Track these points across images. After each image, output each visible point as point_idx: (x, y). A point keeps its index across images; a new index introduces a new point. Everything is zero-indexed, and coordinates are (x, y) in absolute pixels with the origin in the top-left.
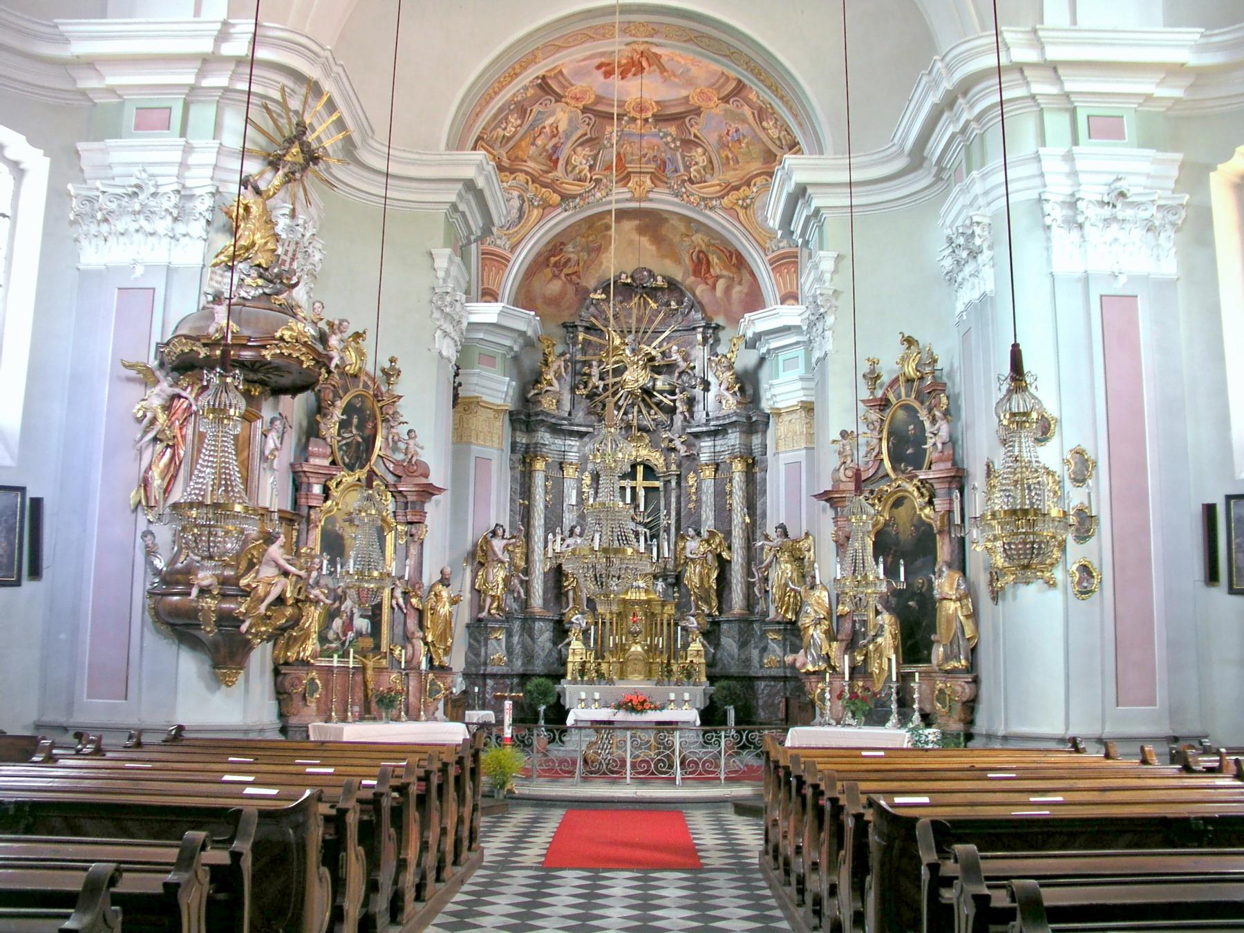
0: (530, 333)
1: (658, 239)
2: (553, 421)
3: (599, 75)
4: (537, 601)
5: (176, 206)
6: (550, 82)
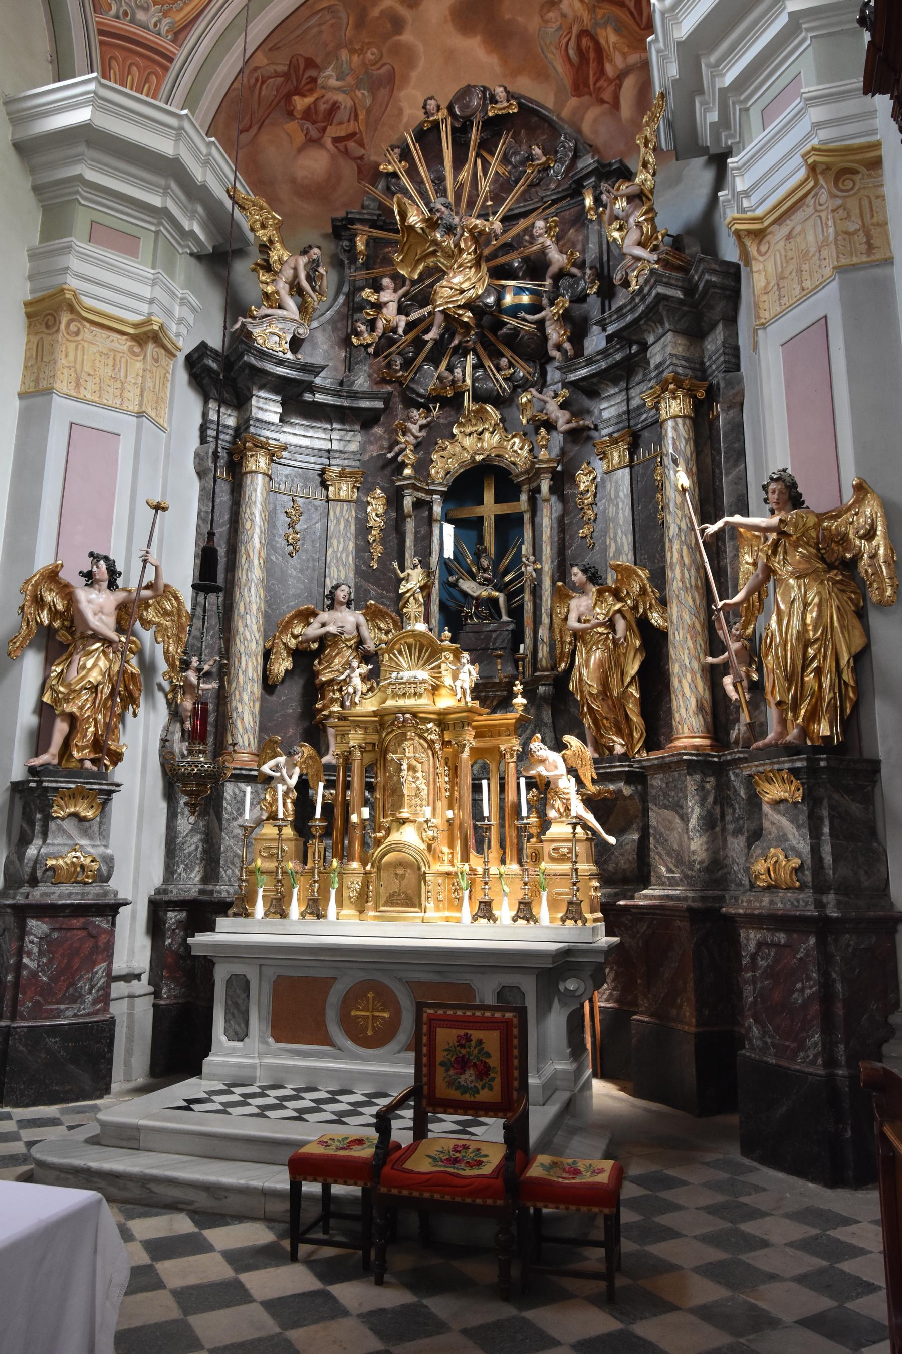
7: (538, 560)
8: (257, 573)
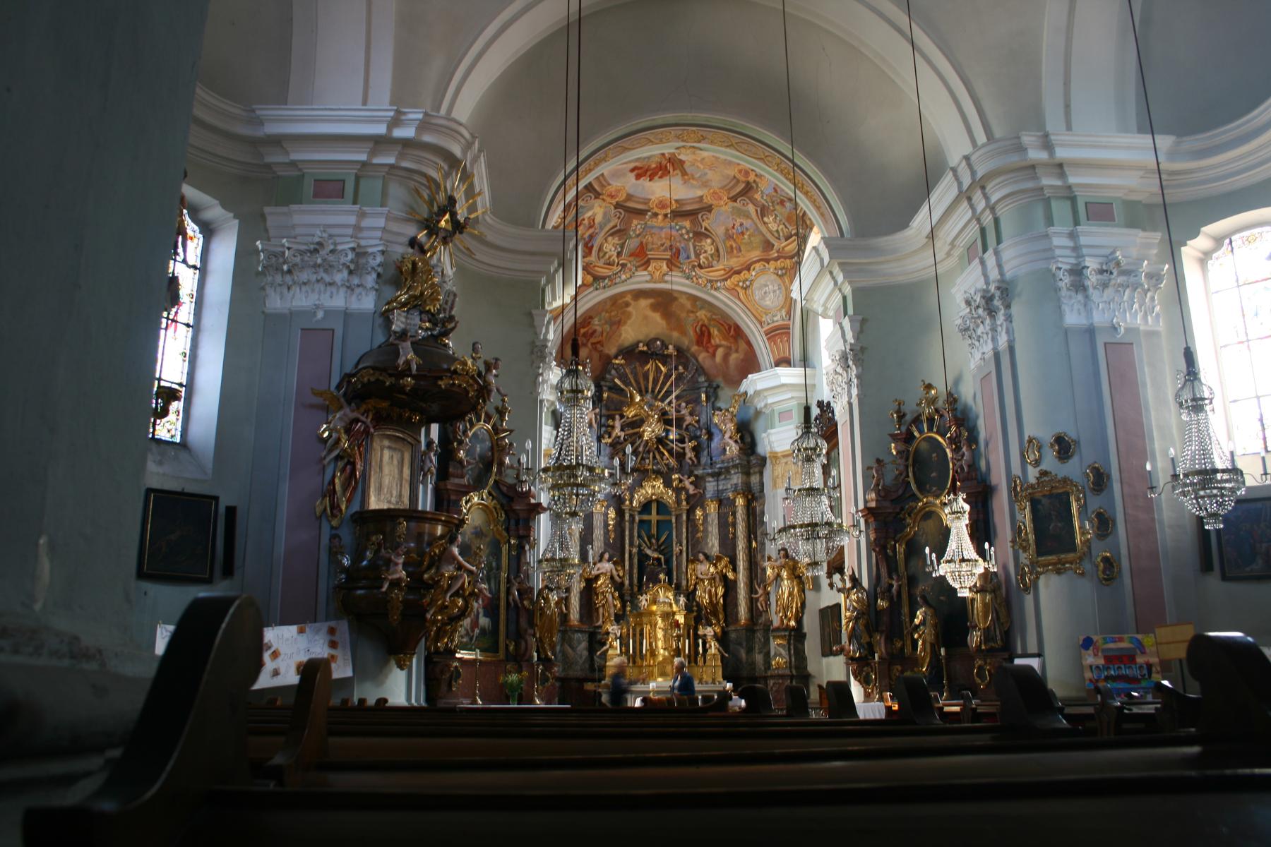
3: (632, 176)
4: (574, 615)
5: (352, 261)
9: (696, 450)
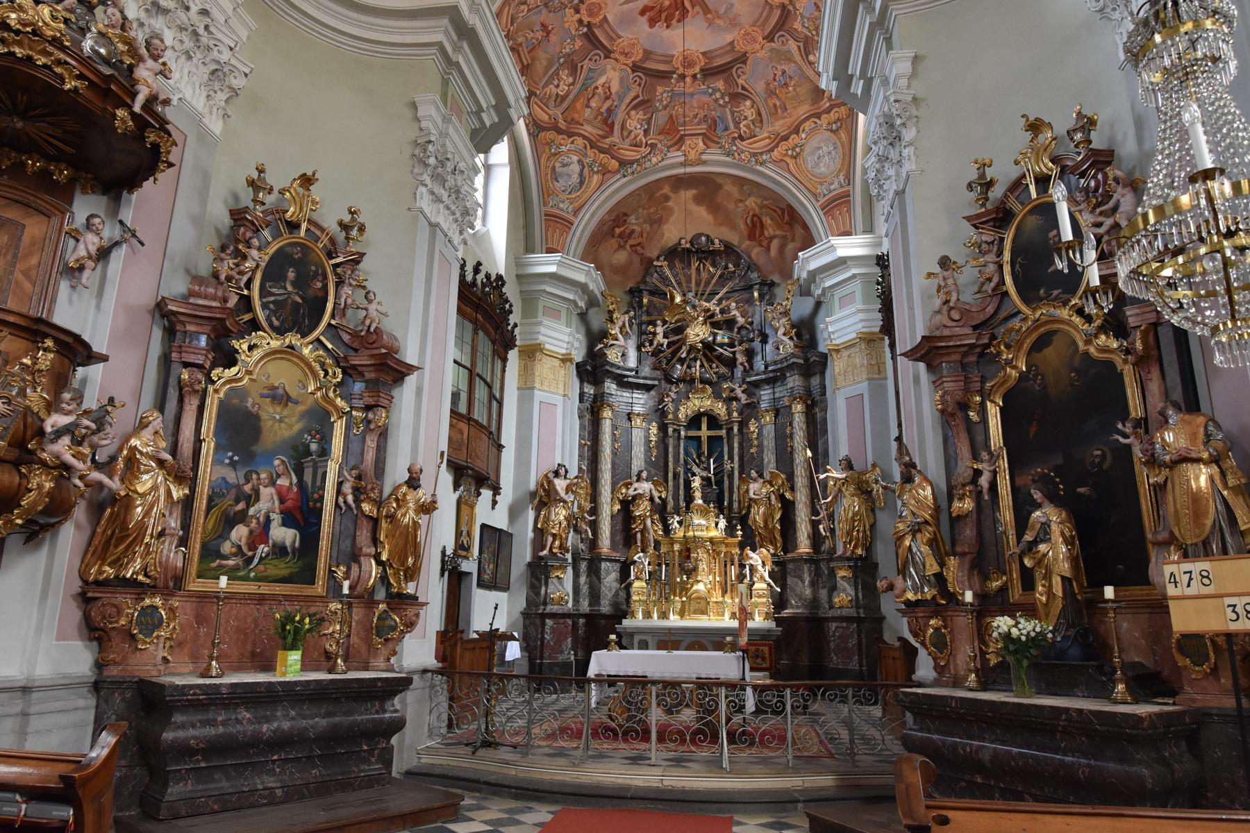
0: (592, 286)
1: (714, 208)
2: (619, 372)
3: (643, 20)
6: (596, 30)
7: (732, 462)
8: (609, 466)
9: (750, 354)
